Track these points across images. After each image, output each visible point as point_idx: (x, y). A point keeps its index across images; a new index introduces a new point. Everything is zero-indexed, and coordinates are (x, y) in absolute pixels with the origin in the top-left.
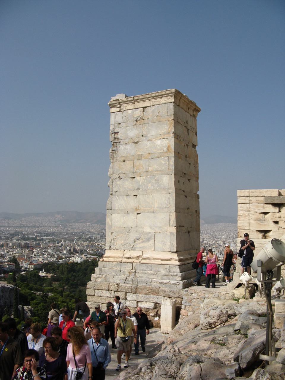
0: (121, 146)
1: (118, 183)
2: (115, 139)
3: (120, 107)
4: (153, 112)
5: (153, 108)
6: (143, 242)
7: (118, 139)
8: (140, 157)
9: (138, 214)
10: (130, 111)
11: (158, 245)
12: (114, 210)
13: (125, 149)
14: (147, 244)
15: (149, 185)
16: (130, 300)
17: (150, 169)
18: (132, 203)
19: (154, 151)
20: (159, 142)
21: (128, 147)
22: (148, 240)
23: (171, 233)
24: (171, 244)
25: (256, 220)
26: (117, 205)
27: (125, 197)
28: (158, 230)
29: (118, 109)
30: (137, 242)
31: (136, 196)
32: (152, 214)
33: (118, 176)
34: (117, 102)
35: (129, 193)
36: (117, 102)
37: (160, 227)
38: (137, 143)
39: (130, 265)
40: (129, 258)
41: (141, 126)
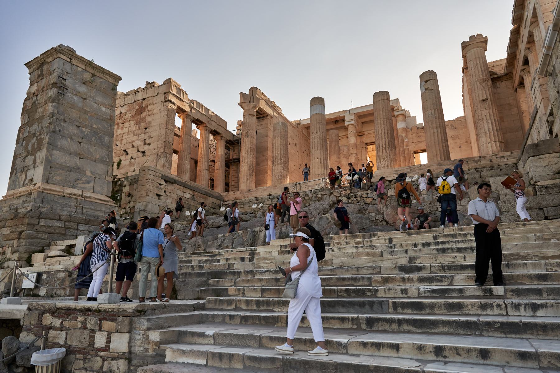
0: (68, 94)
1: (62, 124)
2: (62, 83)
3: (70, 59)
4: (101, 82)
5: (101, 80)
6: (83, 183)
7: (64, 84)
8: (86, 112)
9: (80, 158)
10: (80, 69)
11: (98, 188)
12: (56, 147)
13: (72, 98)
14: (87, 186)
15: (93, 139)
16: (81, 231)
17: (95, 126)
18: (74, 147)
19: (100, 114)
20: (104, 109)
21: (75, 98)
22: (88, 182)
23: (108, 181)
24: (108, 190)
25: (157, 187)
26: (59, 143)
27: (69, 139)
28: (98, 177)
29: (69, 60)
30: (78, 182)
31: (80, 143)
32: (94, 163)
33: (63, 118)
34: (71, 53)
35: (73, 137)
36: (71, 53)
37: (99, 175)
38: (85, 99)
39: (75, 201)
40: (71, 194)
41: (89, 88)
